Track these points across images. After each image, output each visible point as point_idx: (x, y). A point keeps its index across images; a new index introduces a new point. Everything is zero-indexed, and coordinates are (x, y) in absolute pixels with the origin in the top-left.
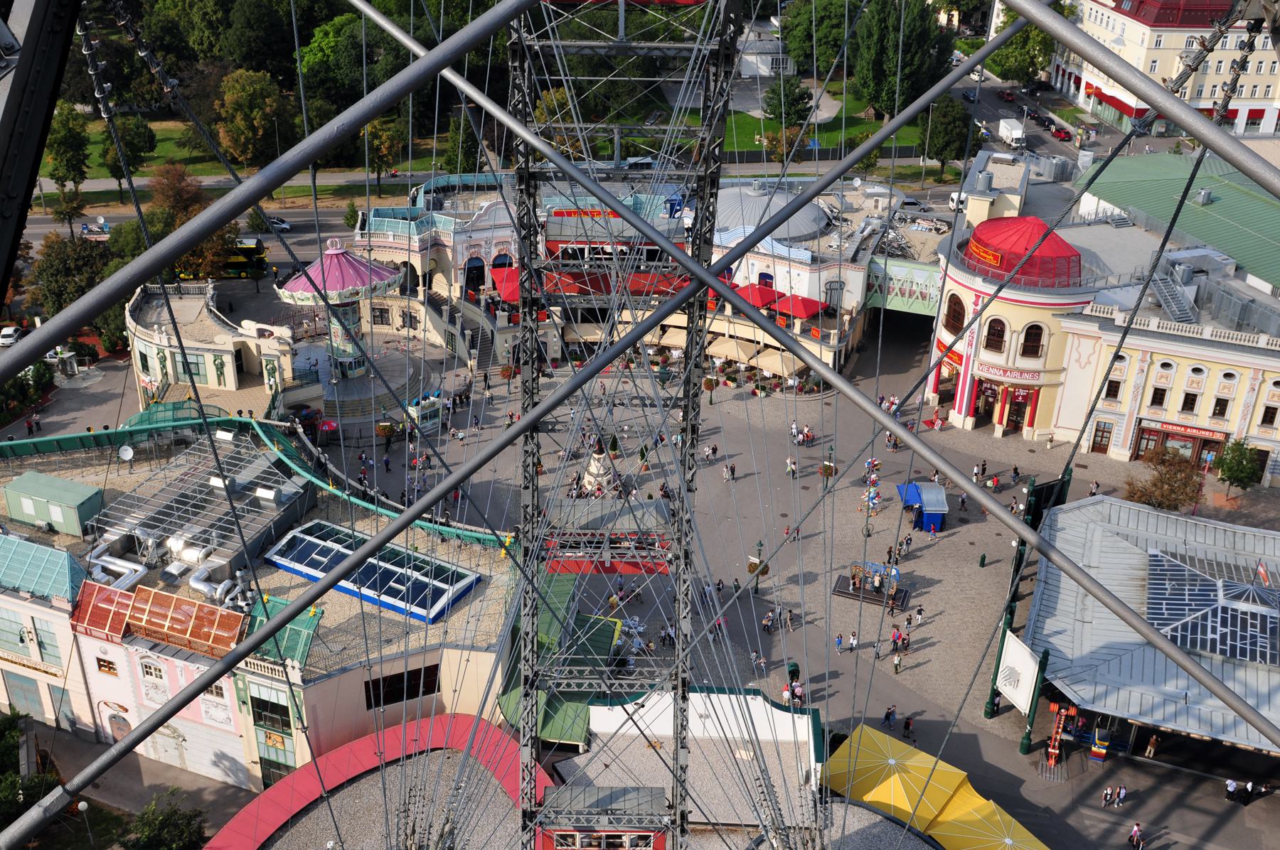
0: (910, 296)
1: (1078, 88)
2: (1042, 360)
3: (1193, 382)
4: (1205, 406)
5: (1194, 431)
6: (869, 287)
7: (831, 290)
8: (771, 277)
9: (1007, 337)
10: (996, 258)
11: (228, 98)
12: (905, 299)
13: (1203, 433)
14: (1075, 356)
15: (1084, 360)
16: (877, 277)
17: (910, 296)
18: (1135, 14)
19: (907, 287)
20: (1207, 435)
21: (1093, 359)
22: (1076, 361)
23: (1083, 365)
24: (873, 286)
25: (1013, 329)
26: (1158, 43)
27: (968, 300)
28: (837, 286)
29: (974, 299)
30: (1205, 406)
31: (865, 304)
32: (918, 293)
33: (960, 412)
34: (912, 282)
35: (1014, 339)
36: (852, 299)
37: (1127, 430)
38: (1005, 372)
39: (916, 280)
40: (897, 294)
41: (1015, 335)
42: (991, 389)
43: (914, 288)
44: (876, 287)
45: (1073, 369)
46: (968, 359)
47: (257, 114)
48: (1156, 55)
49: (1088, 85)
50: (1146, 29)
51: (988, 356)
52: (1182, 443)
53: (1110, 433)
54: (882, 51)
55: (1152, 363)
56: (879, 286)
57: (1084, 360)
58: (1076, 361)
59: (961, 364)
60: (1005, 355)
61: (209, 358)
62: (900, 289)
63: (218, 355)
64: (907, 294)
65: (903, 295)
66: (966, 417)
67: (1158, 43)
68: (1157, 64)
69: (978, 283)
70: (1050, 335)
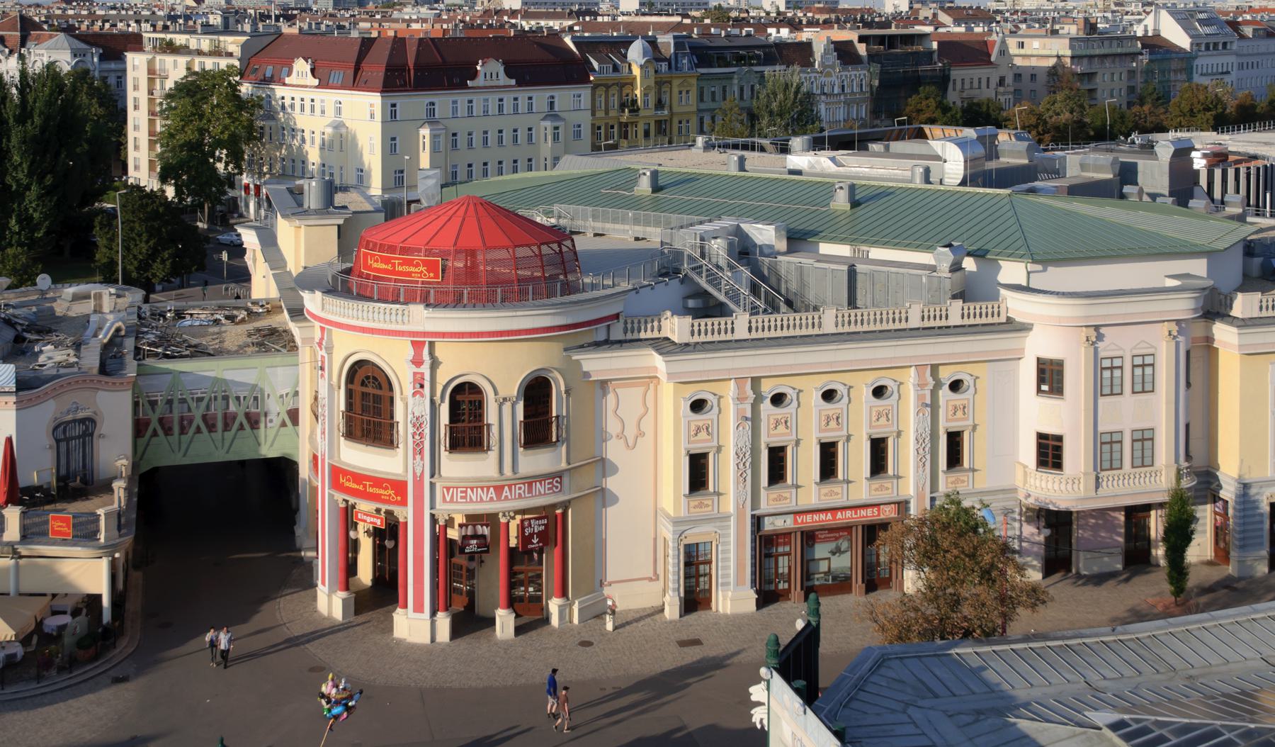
0: (227, 427)
3: (828, 419)
4: (855, 460)
5: (848, 513)
6: (140, 428)
7: (68, 440)
9: (491, 416)
12: (218, 435)
13: (863, 512)
16: (153, 404)
17: (227, 427)
18: (356, 82)
19: (217, 410)
20: (869, 515)
21: (647, 425)
23: (631, 443)
24: (147, 423)
25: (502, 394)
28: (78, 430)
29: (410, 352)
30: (855, 460)
32: (241, 418)
33: (419, 608)
34: (226, 398)
37: (739, 544)
38: (499, 489)
40: (198, 430)
41: (507, 408)
42: (475, 536)
43: (233, 408)
44: (154, 424)
46: (419, 483)
51: (457, 466)
52: (832, 546)
53: (710, 562)
55: (759, 399)
56: (161, 420)
57: (630, 432)
59: (404, 503)
60: (493, 455)
62: (204, 417)
64: (220, 425)
65: (211, 428)
66: (433, 613)
68: (398, 141)
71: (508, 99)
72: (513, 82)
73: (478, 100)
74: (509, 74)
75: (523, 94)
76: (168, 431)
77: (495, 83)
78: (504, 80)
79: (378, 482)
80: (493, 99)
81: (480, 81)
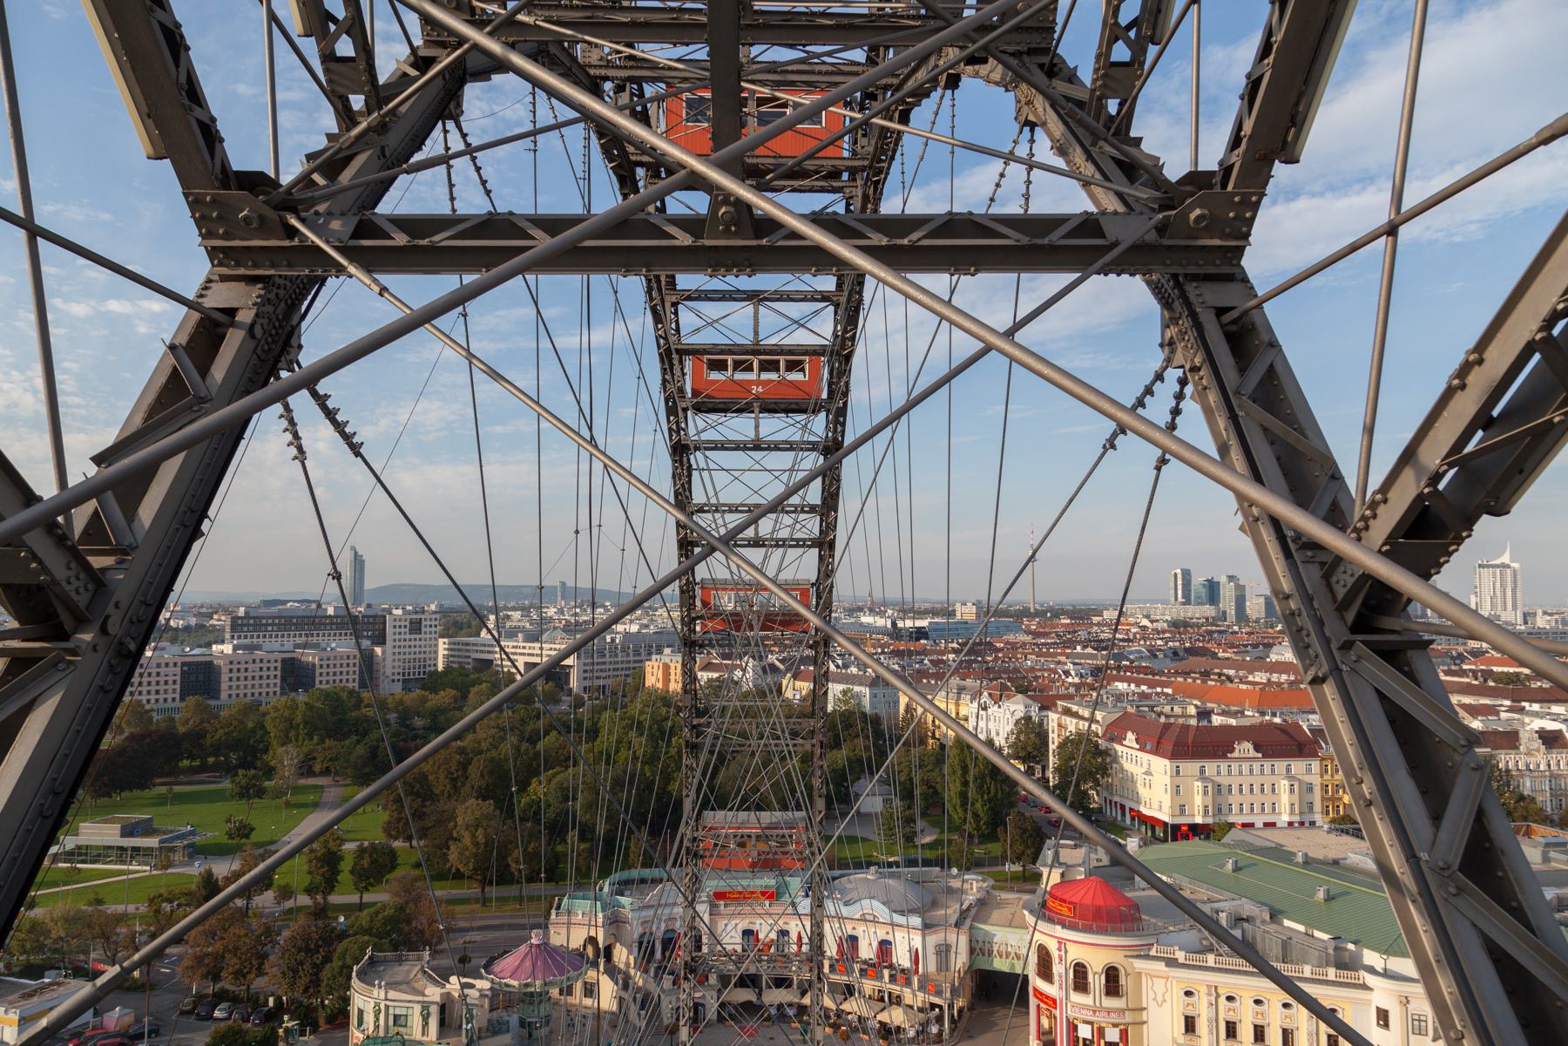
1: (1123, 814)
2: (1124, 999)
6: (972, 951)
8: (890, 943)
10: (1069, 909)
11: (460, 820)
14: (1151, 995)
15: (1160, 999)
18: (1157, 751)
19: (1003, 948)
21: (1168, 996)
22: (1155, 999)
26: (1178, 772)
27: (1052, 946)
31: (970, 967)
35: (1097, 981)
36: (960, 960)
38: (1094, 1012)
39: (1010, 942)
45: (1152, 1006)
47: (480, 832)
48: (1178, 781)
49: (1131, 810)
50: (1167, 762)
51: (1076, 997)
54: (966, 783)
55: (1218, 996)
57: (1160, 999)
58: (1155, 999)
60: (1091, 996)
61: (417, 1008)
63: (425, 1007)
65: (1001, 956)
67: (1178, 772)
69: (1059, 931)
70: (1127, 975)
71: (1257, 765)
72: (1260, 755)
73: (1235, 766)
74: (1257, 749)
75: (1267, 765)
76: (983, 954)
77: (1247, 755)
78: (1253, 753)
79: (1047, 997)
80: (1245, 766)
81: (1236, 754)
